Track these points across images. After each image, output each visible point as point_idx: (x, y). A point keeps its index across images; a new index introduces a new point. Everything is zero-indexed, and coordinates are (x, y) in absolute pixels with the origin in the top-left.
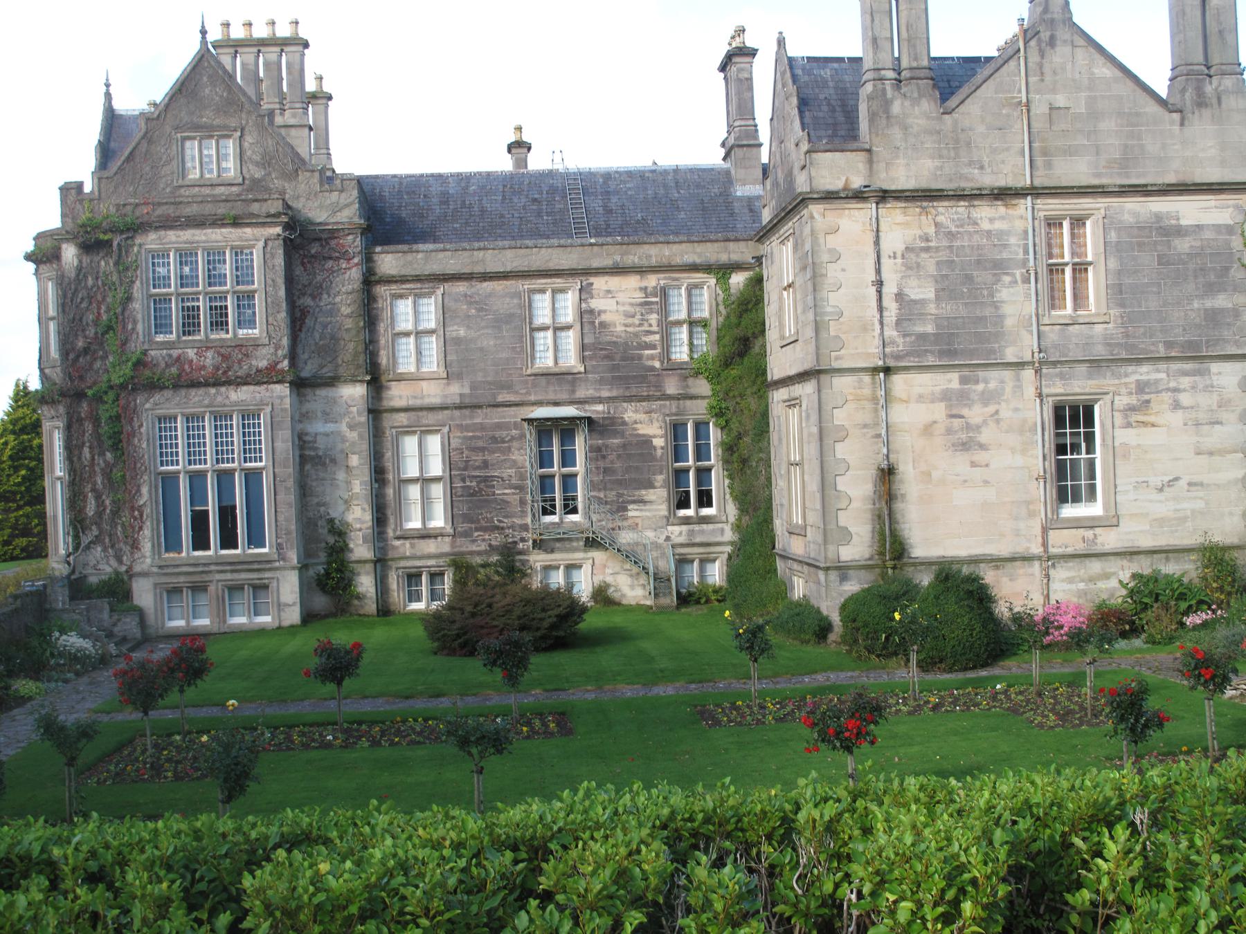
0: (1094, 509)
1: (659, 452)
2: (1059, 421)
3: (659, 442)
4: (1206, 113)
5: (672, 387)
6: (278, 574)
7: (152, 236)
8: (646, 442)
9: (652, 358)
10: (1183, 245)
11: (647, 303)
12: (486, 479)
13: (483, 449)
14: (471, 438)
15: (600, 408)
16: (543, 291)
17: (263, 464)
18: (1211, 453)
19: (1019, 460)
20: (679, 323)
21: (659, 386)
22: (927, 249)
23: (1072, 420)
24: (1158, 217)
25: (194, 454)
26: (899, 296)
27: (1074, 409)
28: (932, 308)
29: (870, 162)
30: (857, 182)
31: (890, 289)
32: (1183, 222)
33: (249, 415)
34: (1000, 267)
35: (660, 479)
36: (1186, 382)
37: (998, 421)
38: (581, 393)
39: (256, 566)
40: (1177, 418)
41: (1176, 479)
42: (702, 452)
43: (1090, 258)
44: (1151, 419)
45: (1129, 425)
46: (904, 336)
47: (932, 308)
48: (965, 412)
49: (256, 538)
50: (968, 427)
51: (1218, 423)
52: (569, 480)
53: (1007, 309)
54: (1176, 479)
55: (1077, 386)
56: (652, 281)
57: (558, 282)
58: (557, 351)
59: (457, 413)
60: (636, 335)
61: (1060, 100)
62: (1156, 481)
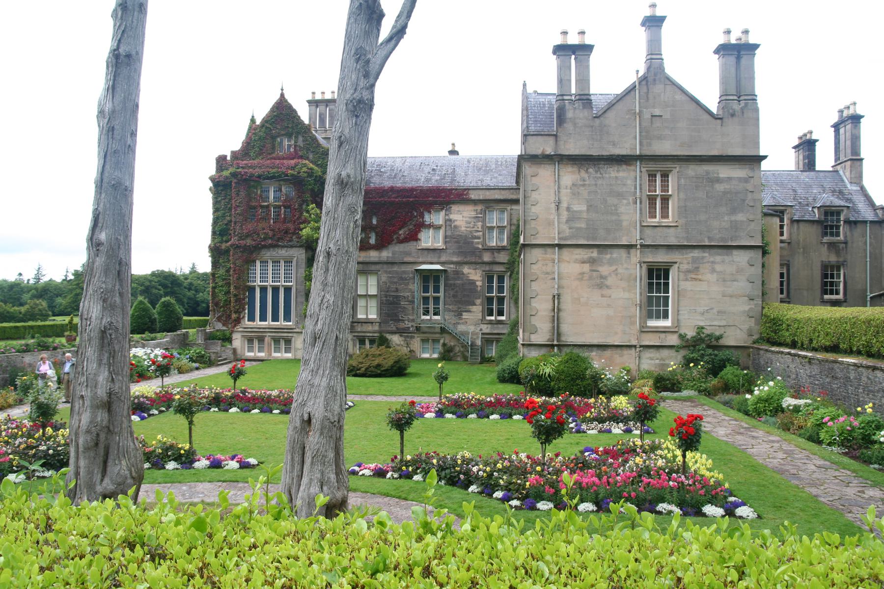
0: (668, 323)
1: (479, 288)
2: (650, 277)
3: (479, 284)
4: (736, 119)
5: (487, 257)
6: (295, 335)
8: (473, 282)
9: (478, 243)
10: (720, 187)
12: (397, 297)
15: (452, 266)
18: (731, 296)
19: (627, 295)
20: (492, 228)
21: (480, 257)
22: (584, 185)
23: (658, 276)
24: (708, 173)
25: (264, 278)
26: (568, 209)
27: (658, 270)
28: (585, 215)
29: (556, 141)
30: (549, 151)
31: (564, 205)
32: (721, 176)
33: (288, 262)
34: (620, 195)
35: (478, 301)
36: (718, 258)
37: (617, 275)
38: (444, 259)
40: (712, 278)
41: (712, 309)
42: (501, 289)
43: (670, 193)
44: (700, 277)
45: (686, 280)
46: (570, 228)
48: (600, 269)
49: (287, 318)
50: (602, 277)
51: (734, 281)
52: (436, 300)
53: (624, 217)
54: (712, 309)
55: (661, 257)
56: (479, 207)
59: (385, 266)
60: (471, 232)
61: (657, 112)
62: (701, 309)
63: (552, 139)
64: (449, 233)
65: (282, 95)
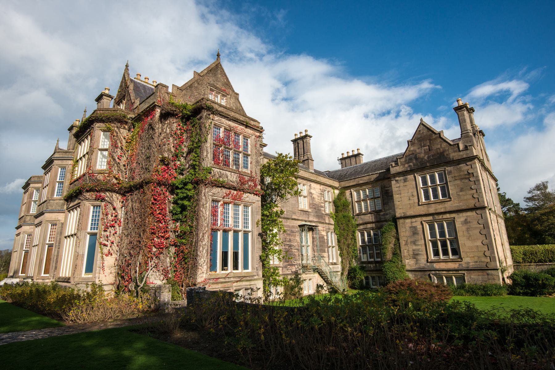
3: (325, 237)
7: (216, 118)
11: (321, 194)
12: (290, 246)
20: (326, 201)
38: (311, 219)
39: (248, 278)
57: (304, 182)
64: (311, 202)
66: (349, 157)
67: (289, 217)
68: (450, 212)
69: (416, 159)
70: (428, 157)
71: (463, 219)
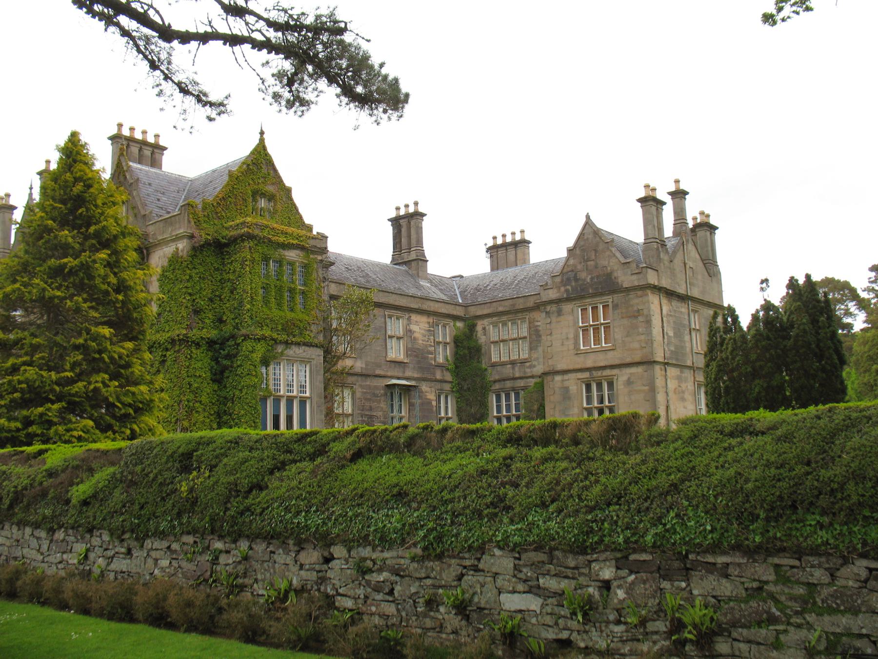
3: (434, 403)
9: (431, 359)
11: (429, 331)
13: (370, 400)
14: (365, 393)
16: (390, 317)
17: (308, 394)
20: (439, 343)
21: (434, 374)
34: (684, 326)
38: (408, 373)
47: (673, 340)
57: (399, 314)
58: (396, 351)
59: (360, 378)
60: (426, 345)
63: (655, 273)
64: (410, 346)
65: (262, 143)
66: (505, 245)
67: (370, 372)
68: (612, 367)
69: (576, 279)
70: (592, 279)
71: (625, 378)
